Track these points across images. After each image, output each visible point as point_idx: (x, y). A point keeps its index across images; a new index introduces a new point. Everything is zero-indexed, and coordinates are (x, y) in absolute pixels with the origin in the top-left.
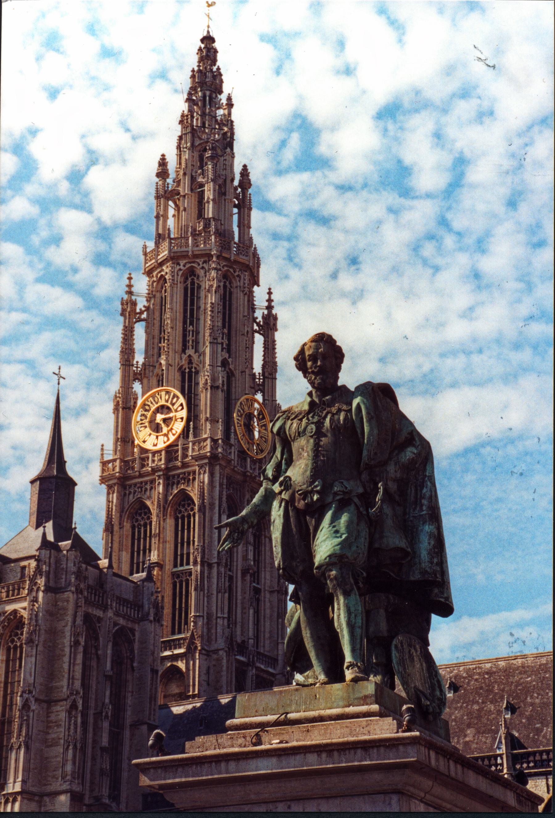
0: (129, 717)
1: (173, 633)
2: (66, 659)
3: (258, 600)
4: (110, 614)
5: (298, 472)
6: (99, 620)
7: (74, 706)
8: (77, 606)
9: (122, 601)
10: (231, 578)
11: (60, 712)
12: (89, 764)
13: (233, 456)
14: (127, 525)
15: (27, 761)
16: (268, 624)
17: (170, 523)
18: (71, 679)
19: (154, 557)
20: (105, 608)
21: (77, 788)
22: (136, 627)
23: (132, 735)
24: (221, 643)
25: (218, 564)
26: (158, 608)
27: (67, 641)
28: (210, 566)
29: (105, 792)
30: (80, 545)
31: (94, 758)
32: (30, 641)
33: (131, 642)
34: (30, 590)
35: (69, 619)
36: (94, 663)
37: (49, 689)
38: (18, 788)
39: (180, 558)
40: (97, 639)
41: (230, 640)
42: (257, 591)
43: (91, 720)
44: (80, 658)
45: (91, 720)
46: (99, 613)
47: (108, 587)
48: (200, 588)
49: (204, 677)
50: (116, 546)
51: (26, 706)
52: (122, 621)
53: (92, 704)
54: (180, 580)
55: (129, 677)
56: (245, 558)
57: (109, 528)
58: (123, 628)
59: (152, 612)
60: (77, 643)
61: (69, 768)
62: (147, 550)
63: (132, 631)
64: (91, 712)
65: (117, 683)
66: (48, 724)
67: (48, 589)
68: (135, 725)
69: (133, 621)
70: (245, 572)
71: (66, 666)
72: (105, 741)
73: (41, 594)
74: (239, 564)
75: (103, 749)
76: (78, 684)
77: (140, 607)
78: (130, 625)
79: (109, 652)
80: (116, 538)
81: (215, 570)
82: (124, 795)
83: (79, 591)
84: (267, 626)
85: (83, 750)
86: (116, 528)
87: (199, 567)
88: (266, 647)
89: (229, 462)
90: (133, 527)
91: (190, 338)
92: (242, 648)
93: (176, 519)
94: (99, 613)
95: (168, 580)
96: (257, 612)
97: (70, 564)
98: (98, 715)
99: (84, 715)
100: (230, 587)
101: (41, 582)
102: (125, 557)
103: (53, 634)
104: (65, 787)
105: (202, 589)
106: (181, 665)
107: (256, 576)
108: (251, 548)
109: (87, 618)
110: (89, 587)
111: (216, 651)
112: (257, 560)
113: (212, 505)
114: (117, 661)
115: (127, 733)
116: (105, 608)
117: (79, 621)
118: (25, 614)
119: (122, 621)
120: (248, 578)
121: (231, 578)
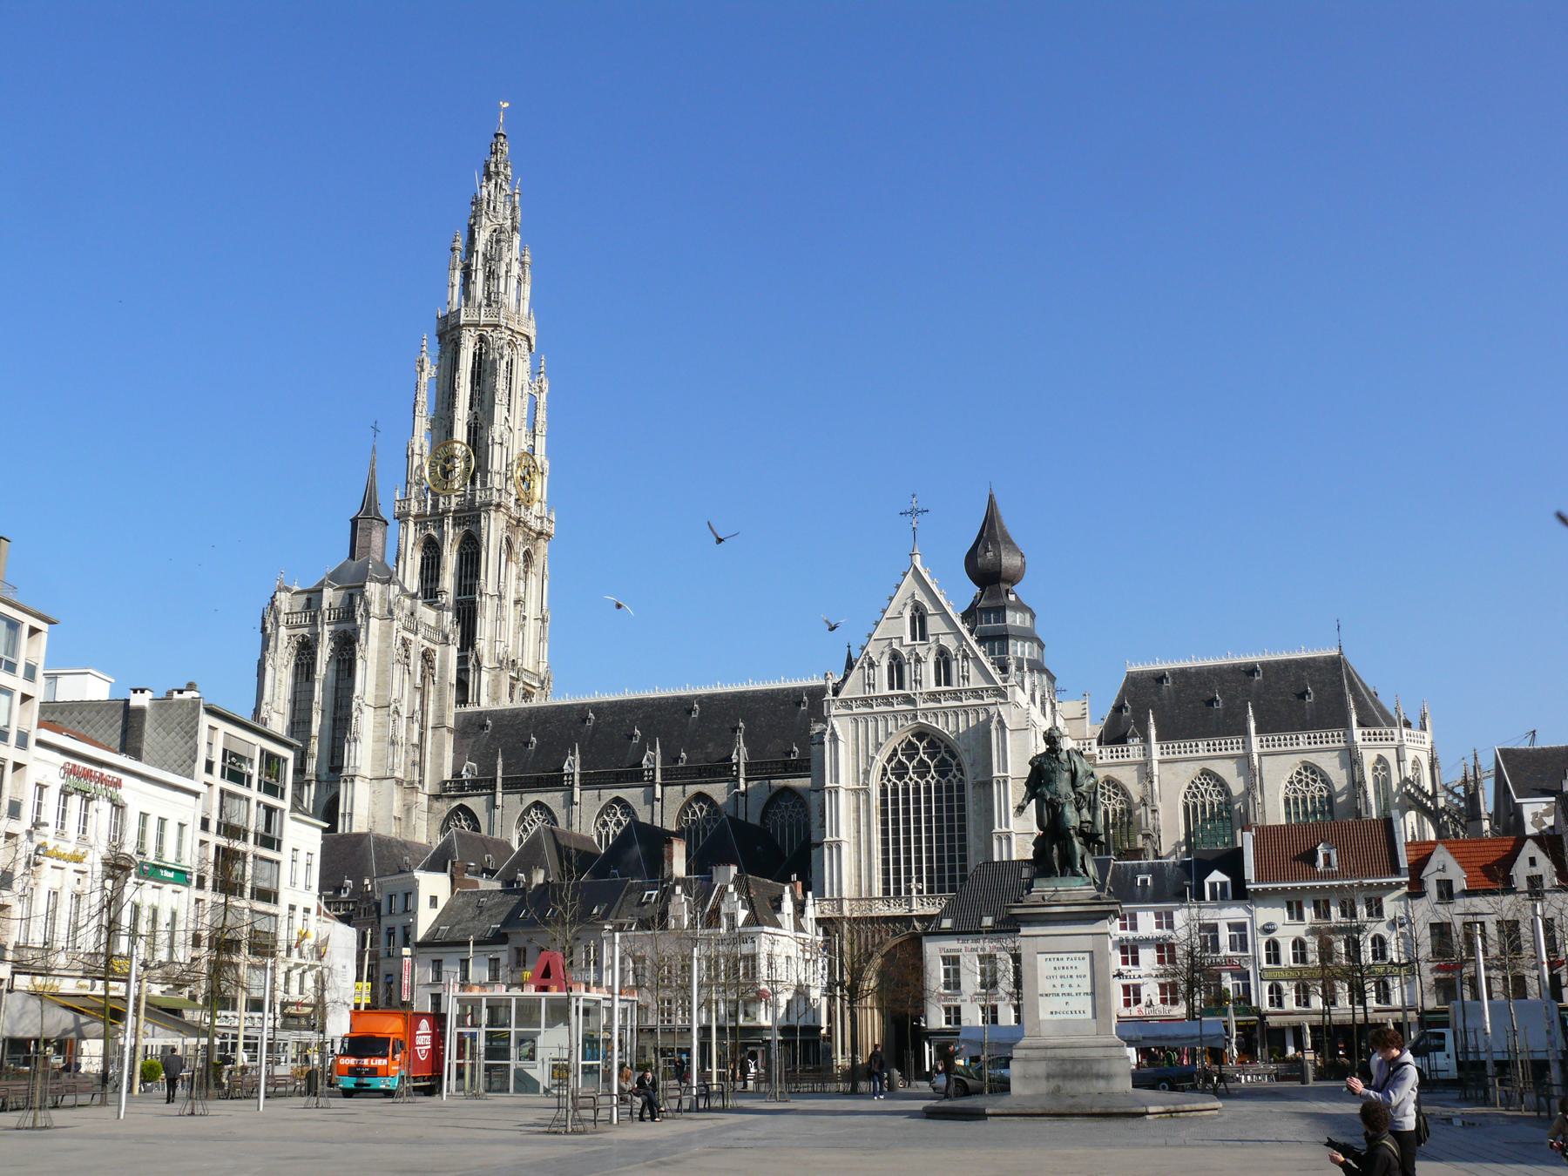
0: (431, 722)
4: (420, 636)
13: (512, 504)
29: (417, 778)
46: (410, 636)
47: (417, 615)
52: (427, 644)
55: (432, 688)
56: (517, 592)
72: (416, 740)
89: (508, 509)
91: (476, 397)
114: (423, 678)
115: (430, 732)
119: (427, 644)
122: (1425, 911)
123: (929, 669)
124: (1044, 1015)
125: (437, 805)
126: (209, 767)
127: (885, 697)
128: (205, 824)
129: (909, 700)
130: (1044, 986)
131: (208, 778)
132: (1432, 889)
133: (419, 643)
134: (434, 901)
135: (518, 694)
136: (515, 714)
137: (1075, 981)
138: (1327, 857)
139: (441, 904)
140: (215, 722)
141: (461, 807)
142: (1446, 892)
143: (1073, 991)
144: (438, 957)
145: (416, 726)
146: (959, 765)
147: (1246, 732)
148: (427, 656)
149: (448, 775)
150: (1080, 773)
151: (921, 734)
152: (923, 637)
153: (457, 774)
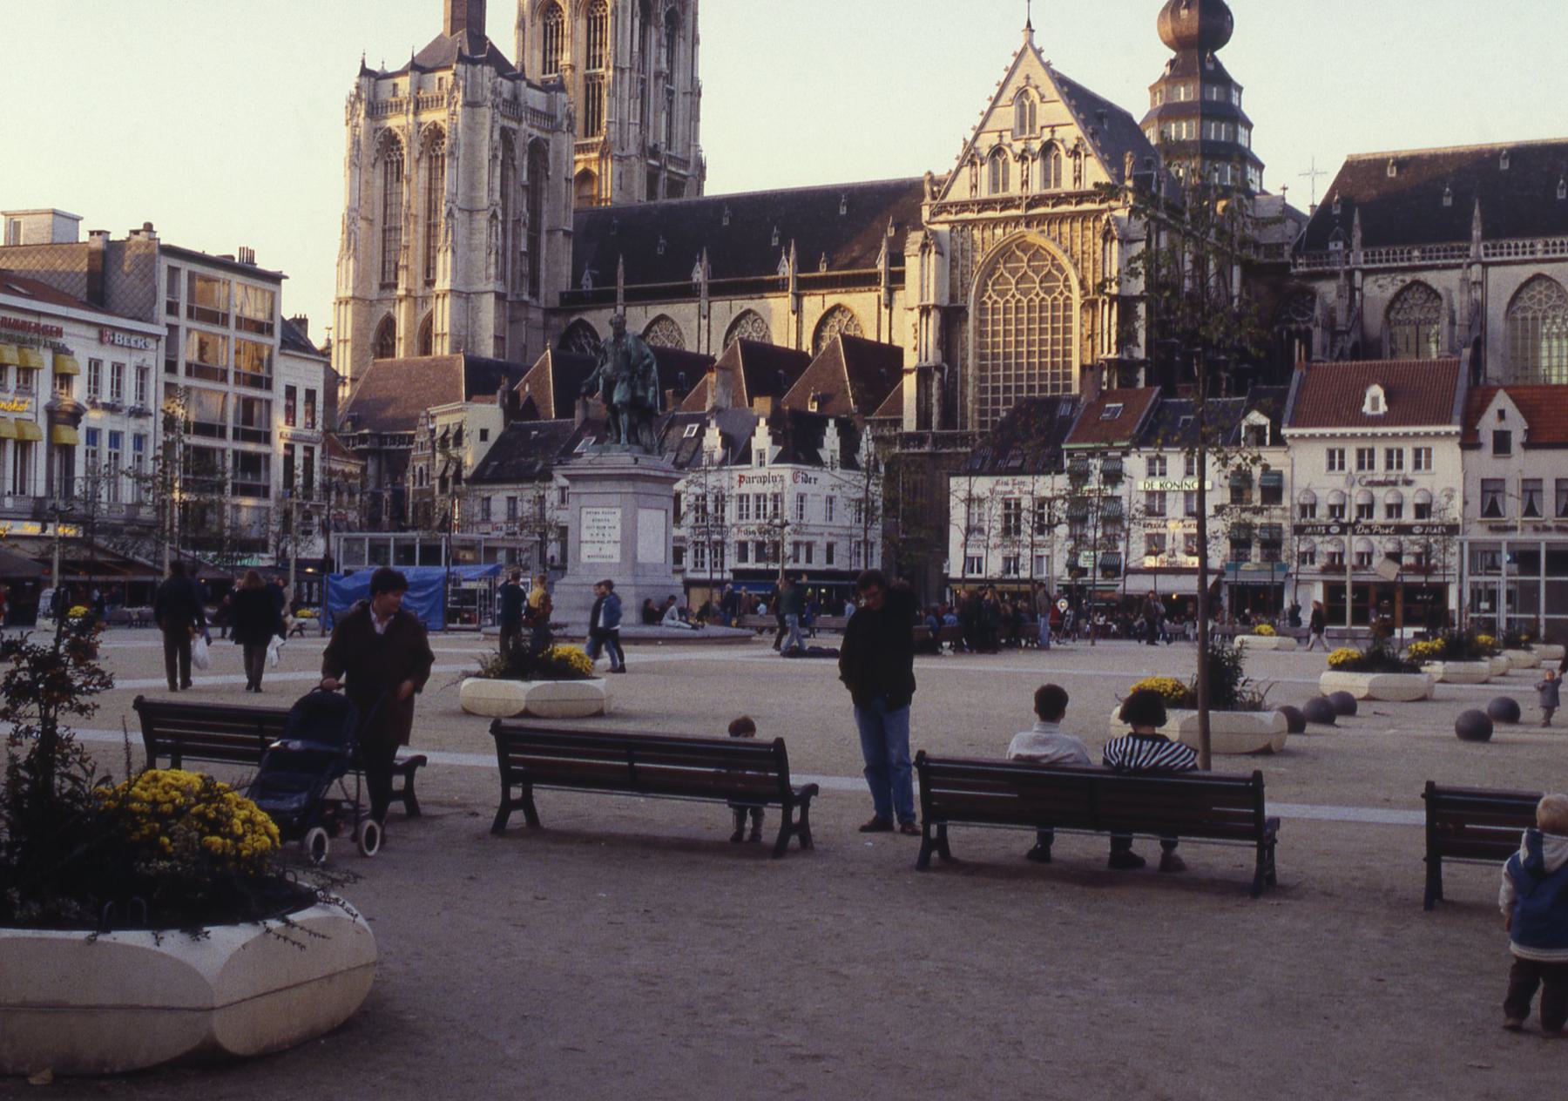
0: (545, 223)
1: (586, 136)
2: (485, 171)
3: (671, 102)
4: (524, 125)
5: (608, 367)
6: (515, 132)
7: (494, 216)
8: (494, 121)
9: (535, 112)
10: (643, 81)
11: (482, 221)
12: (509, 267)
14: (539, 23)
15: (454, 263)
16: (680, 127)
17: (582, 24)
18: (491, 190)
19: (566, 58)
20: (520, 121)
21: (500, 290)
22: (549, 136)
23: (549, 240)
24: (633, 149)
25: (631, 69)
26: (570, 117)
27: (485, 154)
28: (622, 70)
30: (495, 59)
31: (514, 261)
32: (451, 154)
33: (545, 153)
34: (449, 104)
35: (487, 133)
36: (511, 173)
37: (471, 199)
38: (447, 285)
39: (592, 60)
40: (513, 150)
41: (643, 145)
42: (670, 93)
43: (510, 226)
44: (498, 170)
45: (510, 226)
46: (514, 125)
47: (522, 99)
48: (613, 94)
49: (617, 182)
50: (528, 44)
51: (450, 214)
52: (536, 132)
53: (511, 212)
54: (592, 86)
57: (521, 25)
58: (537, 139)
59: (566, 123)
60: (495, 156)
61: (492, 271)
62: (559, 50)
63: (547, 142)
64: (510, 219)
65: (534, 192)
66: (471, 233)
67: (467, 104)
68: (551, 232)
69: (547, 131)
70: (658, 75)
71: (486, 177)
73: (459, 108)
74: (652, 67)
75: (522, 253)
76: (497, 196)
77: (550, 117)
78: (544, 135)
79: (525, 163)
80: (528, 35)
81: (627, 75)
82: (542, 291)
83: (495, 106)
84: (679, 128)
85: (504, 255)
86: (528, 25)
87: (611, 72)
88: (678, 150)
90: (545, 25)
92: (654, 152)
93: (589, 20)
94: (514, 125)
95: (580, 82)
96: (670, 114)
97: (486, 79)
98: (517, 222)
99: (504, 222)
100: (643, 91)
101: (459, 96)
102: (538, 55)
103: (472, 147)
104: (491, 287)
105: (615, 94)
106: (595, 169)
107: (669, 78)
108: (664, 51)
109: (504, 132)
110: (505, 100)
111: (628, 157)
112: (670, 61)
113: (624, 8)
114: (532, 171)
115: (544, 238)
116: (520, 121)
117: (496, 136)
118: (445, 126)
119: (536, 132)
120: (661, 81)
121: (643, 81)
122: (1486, 463)
123: (1037, 167)
124: (584, 559)
125: (554, 321)
126: (172, 309)
127: (985, 205)
128: (171, 367)
129: (1008, 203)
130: (585, 535)
131: (172, 320)
132: (1487, 438)
133: (527, 130)
134: (484, 435)
135: (661, 189)
136: (644, 212)
137: (607, 531)
138: (1375, 400)
139: (494, 436)
140: (175, 263)
141: (581, 321)
142: (1502, 443)
143: (607, 538)
144: (512, 494)
145: (524, 231)
146: (1066, 279)
147: (1468, 237)
148: (537, 151)
149: (565, 283)
150: (634, 354)
151: (1025, 247)
152: (1032, 127)
153: (576, 280)
